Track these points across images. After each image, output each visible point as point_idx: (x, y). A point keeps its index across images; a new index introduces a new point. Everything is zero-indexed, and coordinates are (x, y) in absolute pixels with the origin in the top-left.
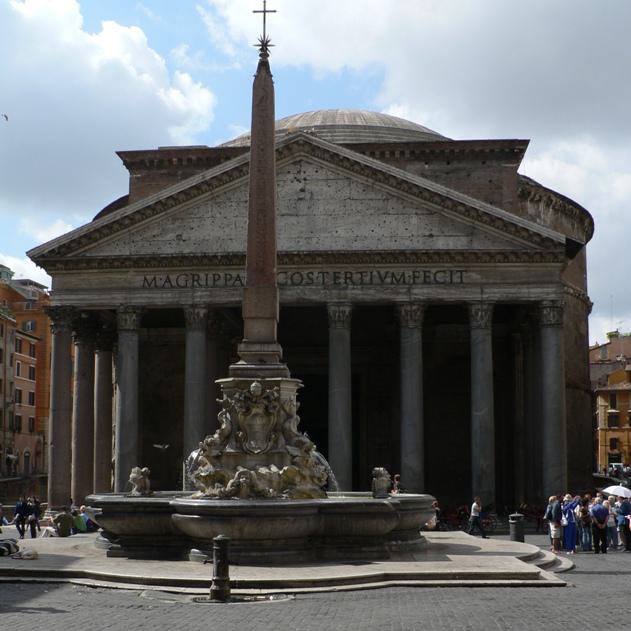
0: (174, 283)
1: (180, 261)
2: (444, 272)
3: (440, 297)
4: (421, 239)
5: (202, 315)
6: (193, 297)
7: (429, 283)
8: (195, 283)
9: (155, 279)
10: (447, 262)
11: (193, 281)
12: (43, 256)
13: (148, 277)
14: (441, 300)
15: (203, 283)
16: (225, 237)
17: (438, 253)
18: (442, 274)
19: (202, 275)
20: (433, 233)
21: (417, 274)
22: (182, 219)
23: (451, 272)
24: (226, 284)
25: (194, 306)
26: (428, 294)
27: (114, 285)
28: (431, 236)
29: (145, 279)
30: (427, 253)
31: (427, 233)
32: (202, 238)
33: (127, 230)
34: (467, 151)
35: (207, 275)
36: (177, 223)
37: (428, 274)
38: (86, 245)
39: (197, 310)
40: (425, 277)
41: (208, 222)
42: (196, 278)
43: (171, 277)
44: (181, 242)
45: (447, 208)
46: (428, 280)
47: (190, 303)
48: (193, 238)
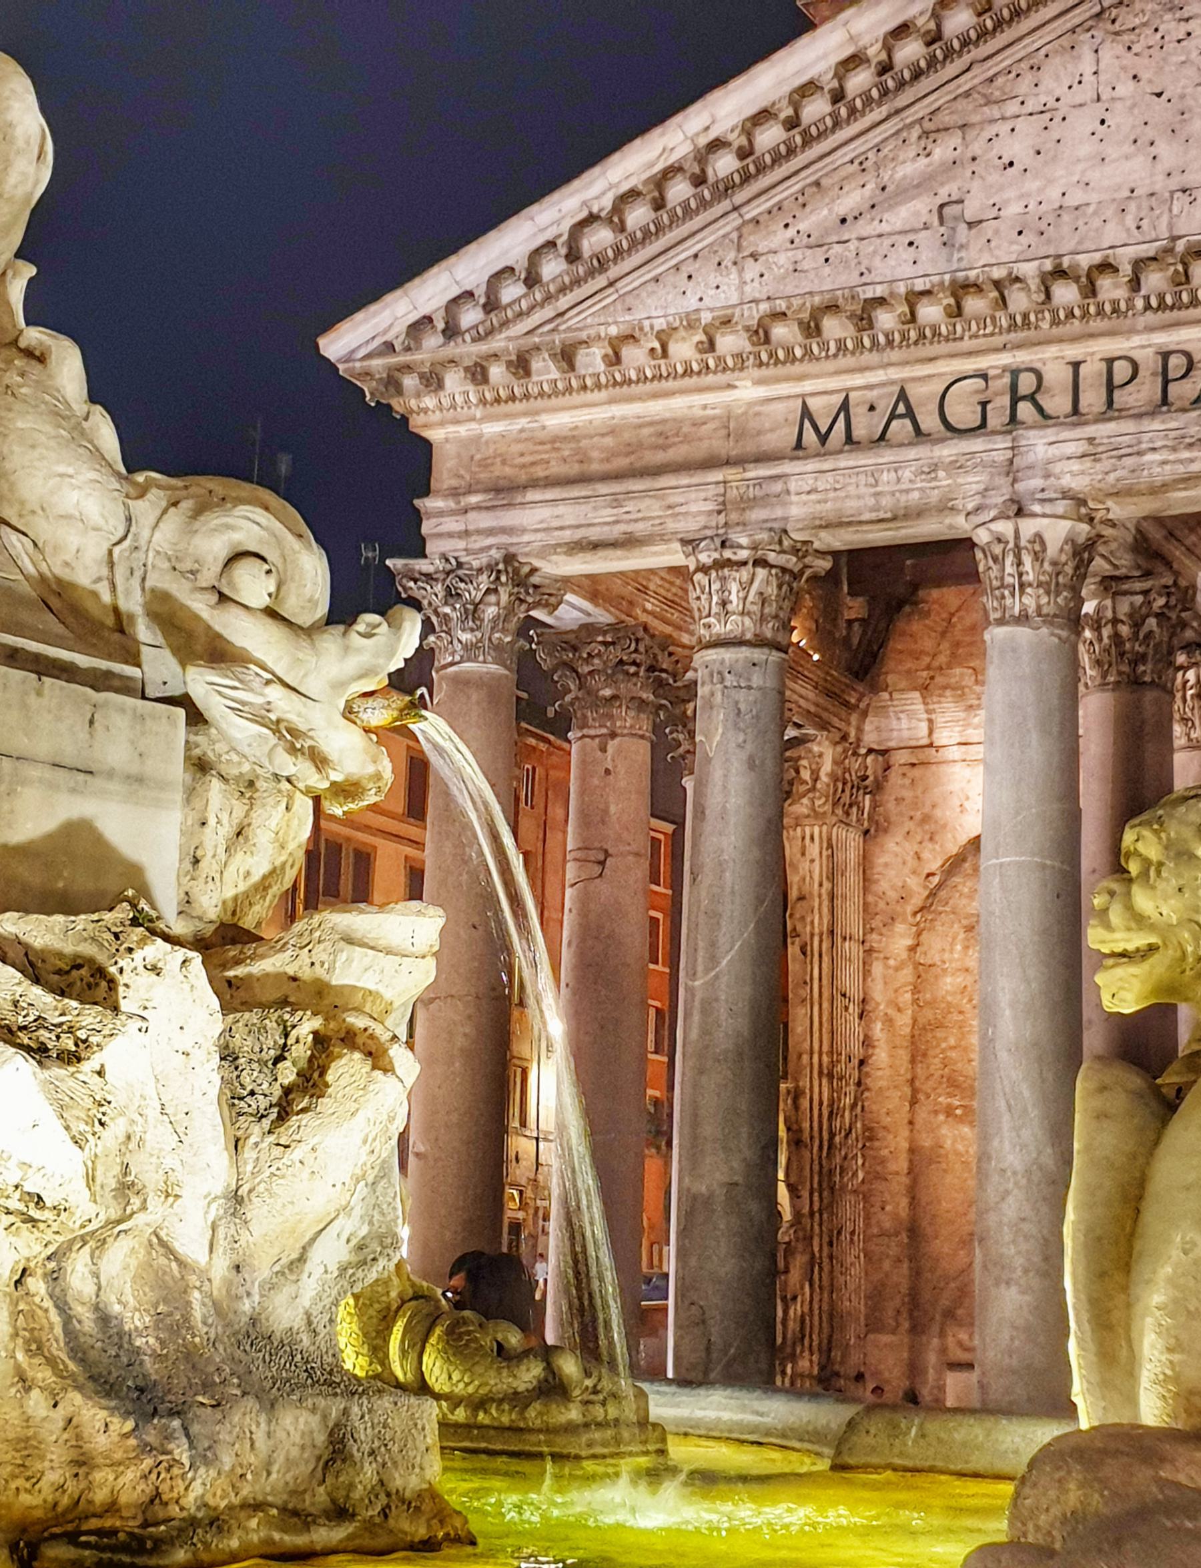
0: (929, 421)
8: (1024, 409)
9: (845, 406)
12: (389, 347)
13: (814, 404)
15: (1058, 403)
16: (1161, 184)
24: (1165, 400)
27: (672, 455)
29: (806, 413)
33: (726, 205)
35: (1076, 365)
36: (942, 151)
38: (563, 290)
41: (1085, 122)
42: (1026, 383)
43: (914, 392)
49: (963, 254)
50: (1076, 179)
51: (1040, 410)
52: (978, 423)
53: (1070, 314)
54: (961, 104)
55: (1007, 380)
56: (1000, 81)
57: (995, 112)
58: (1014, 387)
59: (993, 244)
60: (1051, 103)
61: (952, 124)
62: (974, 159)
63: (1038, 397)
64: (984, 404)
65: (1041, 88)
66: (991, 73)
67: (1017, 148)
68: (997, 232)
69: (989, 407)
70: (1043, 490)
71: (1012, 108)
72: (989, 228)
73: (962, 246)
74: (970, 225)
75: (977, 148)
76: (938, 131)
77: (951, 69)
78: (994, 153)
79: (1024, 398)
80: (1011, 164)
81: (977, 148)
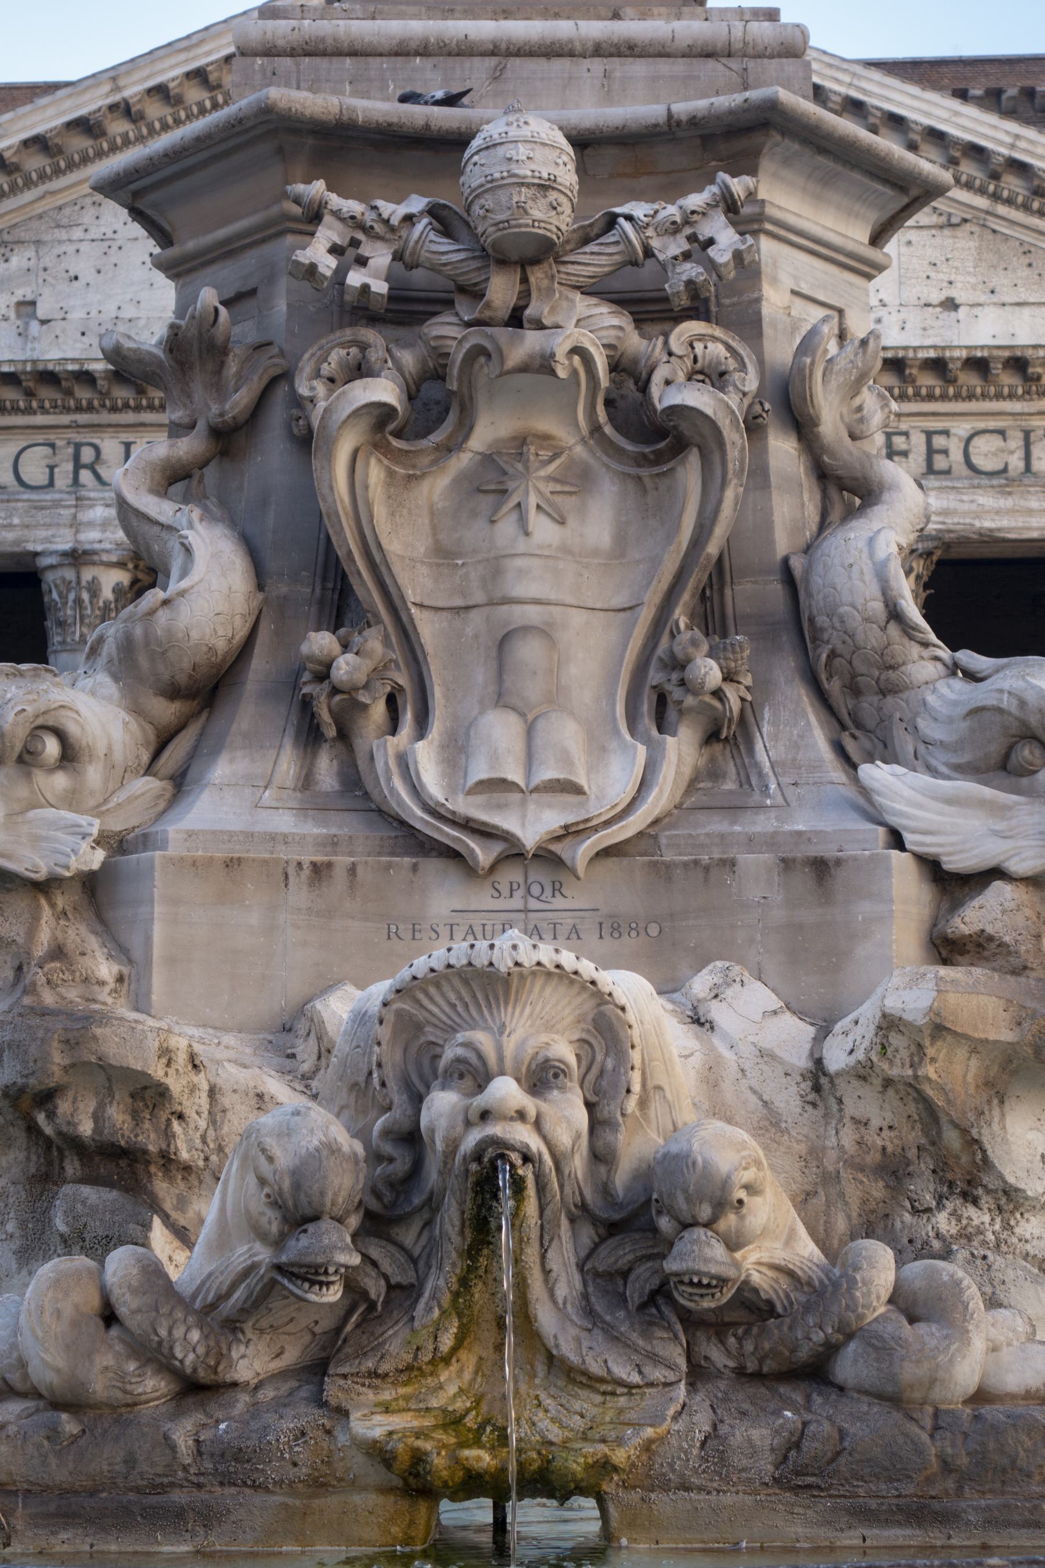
1: (29, 394)
2: (1002, 433)
3: (988, 524)
4: (915, 318)
5: (107, 594)
6: (76, 525)
7: (947, 472)
8: (85, 476)
10: (1012, 396)
11: (78, 466)
14: (988, 538)
17: (979, 365)
18: (996, 441)
19: (110, 446)
20: (959, 295)
21: (899, 442)
22: (38, 243)
23: (1027, 434)
25: (77, 557)
26: (945, 512)
28: (950, 305)
30: (938, 366)
31: (936, 297)
32: (110, 310)
34: (1012, 92)
35: (128, 446)
37: (939, 441)
39: (87, 574)
40: (931, 452)
42: (87, 455)
44: (34, 327)
45: (1009, 202)
46: (940, 462)
47: (67, 547)
48: (77, 315)
49: (36, 345)
50: (129, 297)
51: (98, 477)
52: (25, 477)
53: (126, 406)
54: (35, 224)
55: (71, 450)
56: (67, 211)
57: (63, 234)
58: (77, 457)
59: (60, 340)
60: (110, 235)
61: (27, 238)
62: (45, 270)
63: (98, 468)
64: (52, 468)
65: (102, 221)
66: (59, 203)
67: (83, 267)
68: (64, 331)
69: (56, 470)
70: (100, 541)
71: (77, 233)
72: (57, 327)
73: (34, 338)
74: (44, 322)
75: (48, 260)
76: (16, 242)
77: (28, 196)
78: (64, 266)
79: (85, 467)
80: (76, 278)
81: (48, 260)
